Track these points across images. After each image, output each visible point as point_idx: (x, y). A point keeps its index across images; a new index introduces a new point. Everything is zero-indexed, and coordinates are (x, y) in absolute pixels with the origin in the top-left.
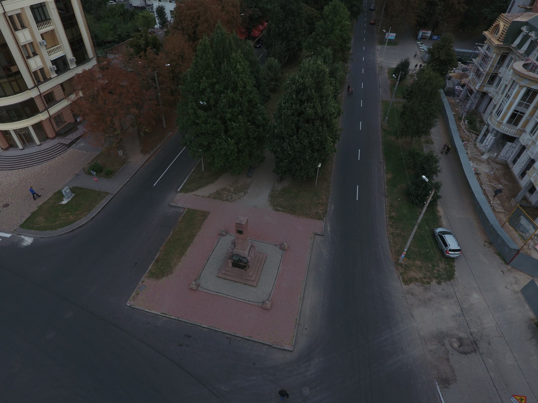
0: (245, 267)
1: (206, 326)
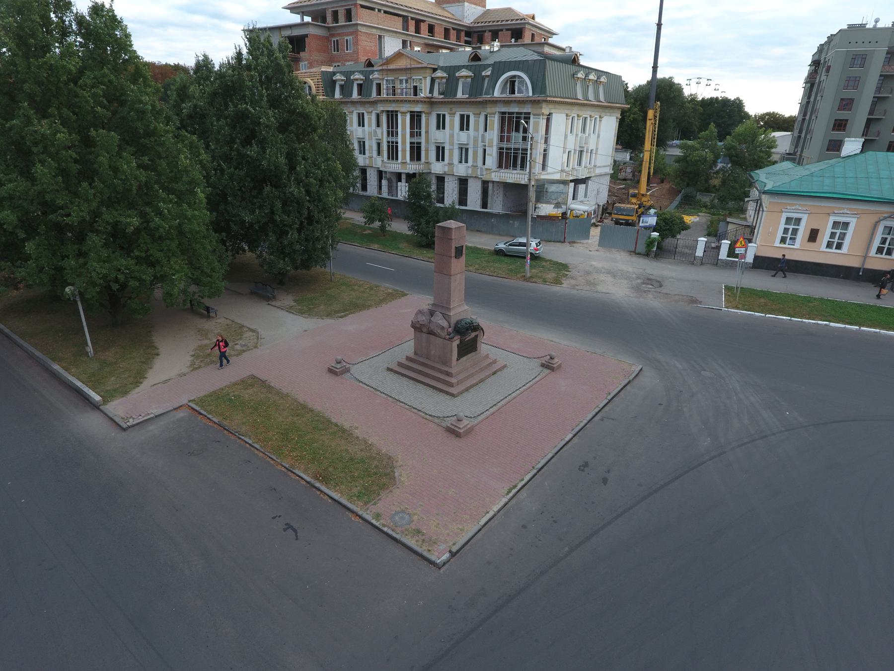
0: (476, 336)
1: (570, 436)
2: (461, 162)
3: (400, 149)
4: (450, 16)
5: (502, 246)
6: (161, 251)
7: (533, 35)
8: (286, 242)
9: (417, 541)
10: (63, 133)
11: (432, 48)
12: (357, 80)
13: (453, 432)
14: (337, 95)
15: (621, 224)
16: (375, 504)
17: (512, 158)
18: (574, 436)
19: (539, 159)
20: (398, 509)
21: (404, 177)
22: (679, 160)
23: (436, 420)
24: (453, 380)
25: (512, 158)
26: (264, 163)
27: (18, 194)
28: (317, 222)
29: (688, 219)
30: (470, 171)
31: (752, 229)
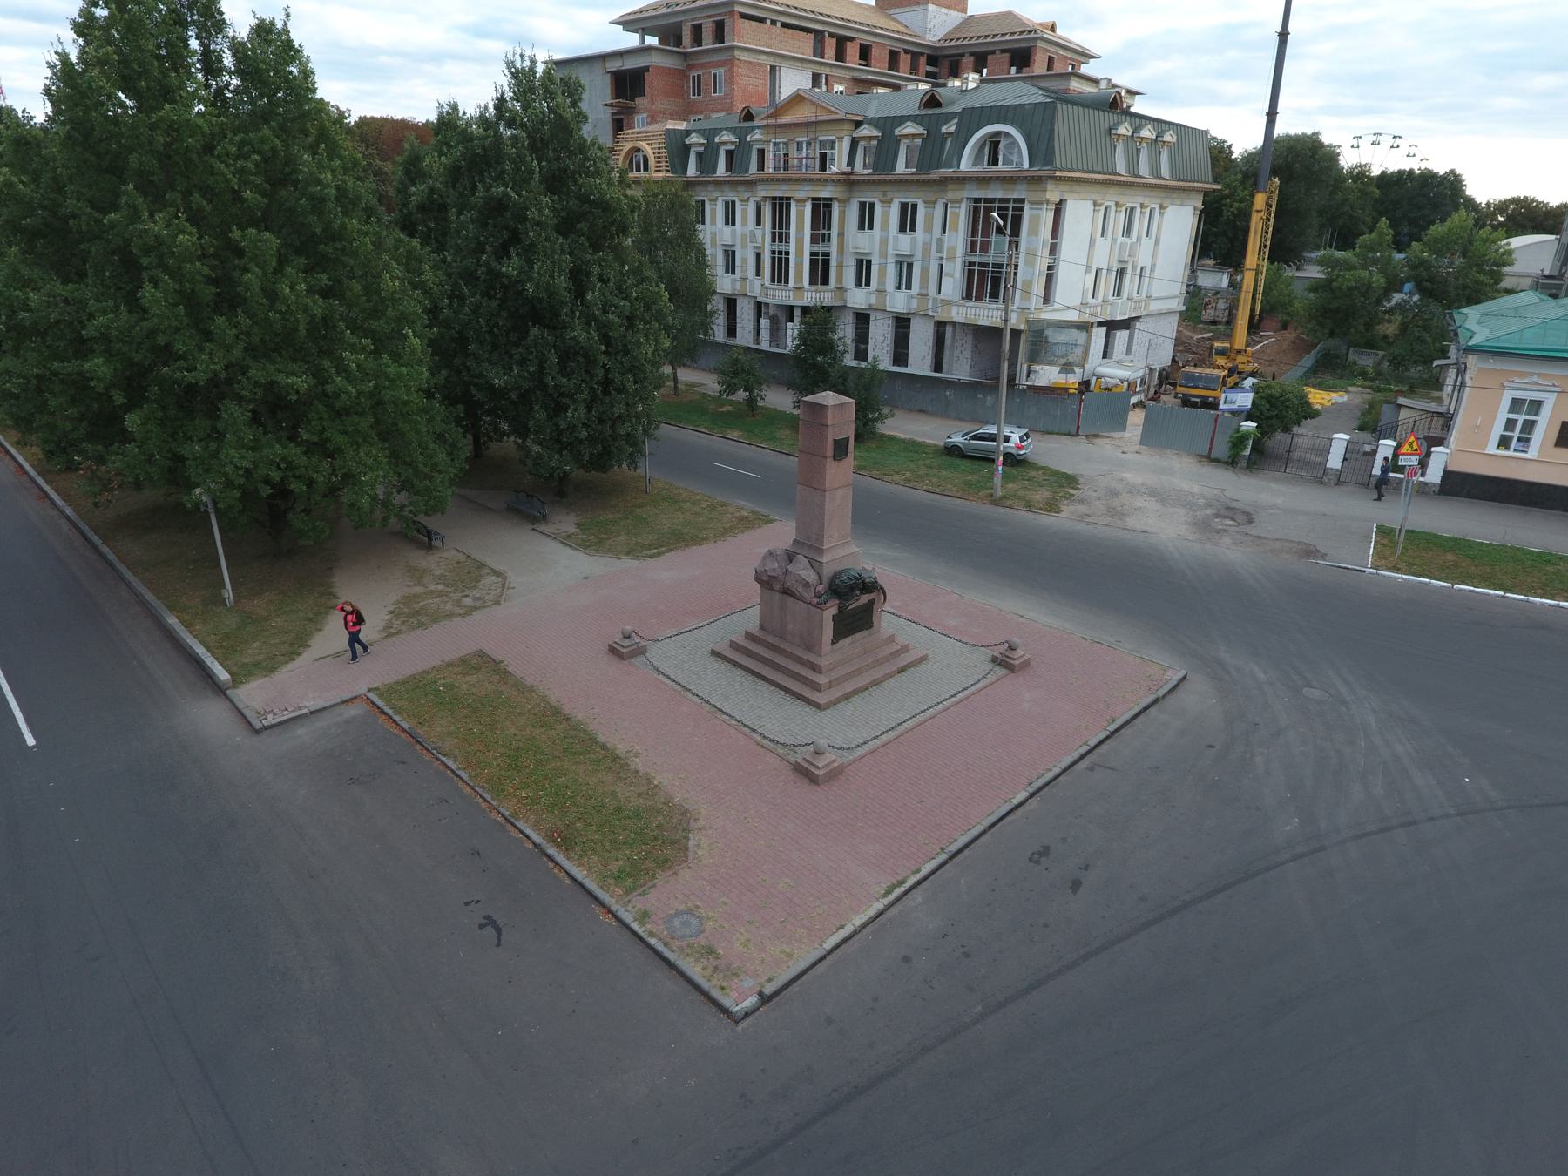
0: (871, 602)
1: (1023, 795)
2: (899, 288)
3: (792, 264)
4: (901, 29)
5: (957, 439)
6: (346, 433)
7: (1051, 60)
8: (563, 425)
9: (704, 968)
10: (190, 234)
11: (863, 85)
12: (725, 143)
13: (805, 773)
14: (692, 171)
15: (1194, 405)
16: (643, 894)
17: (986, 281)
18: (1032, 795)
19: (1039, 287)
20: (682, 907)
21: (797, 313)
22: (1316, 287)
23: (780, 751)
24: (822, 680)
25: (986, 281)
26: (530, 288)
27: (114, 332)
28: (619, 391)
29: (1319, 398)
30: (914, 305)
31: (1448, 420)
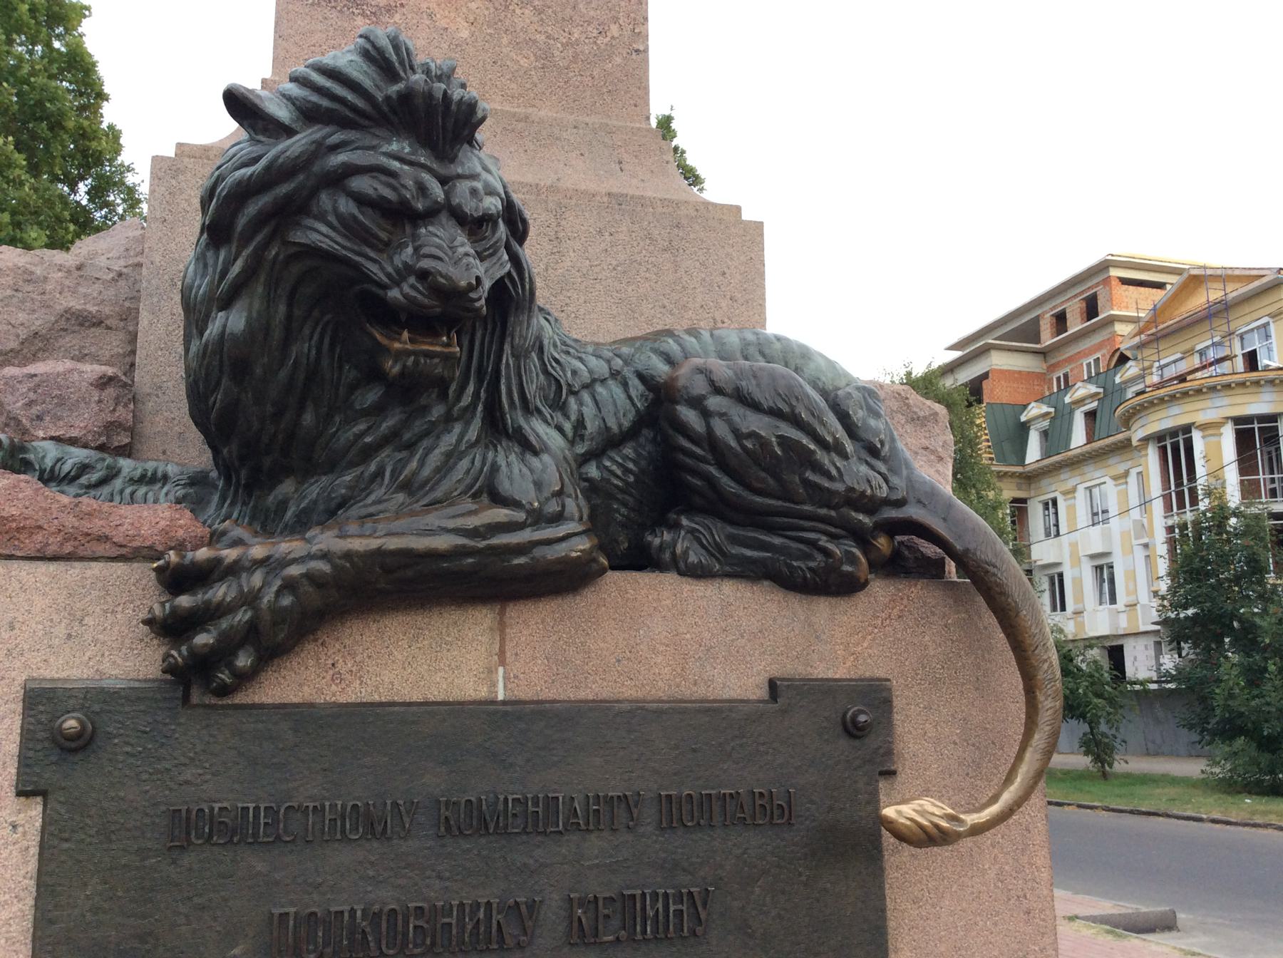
12: (1080, 402)
14: (1033, 452)
